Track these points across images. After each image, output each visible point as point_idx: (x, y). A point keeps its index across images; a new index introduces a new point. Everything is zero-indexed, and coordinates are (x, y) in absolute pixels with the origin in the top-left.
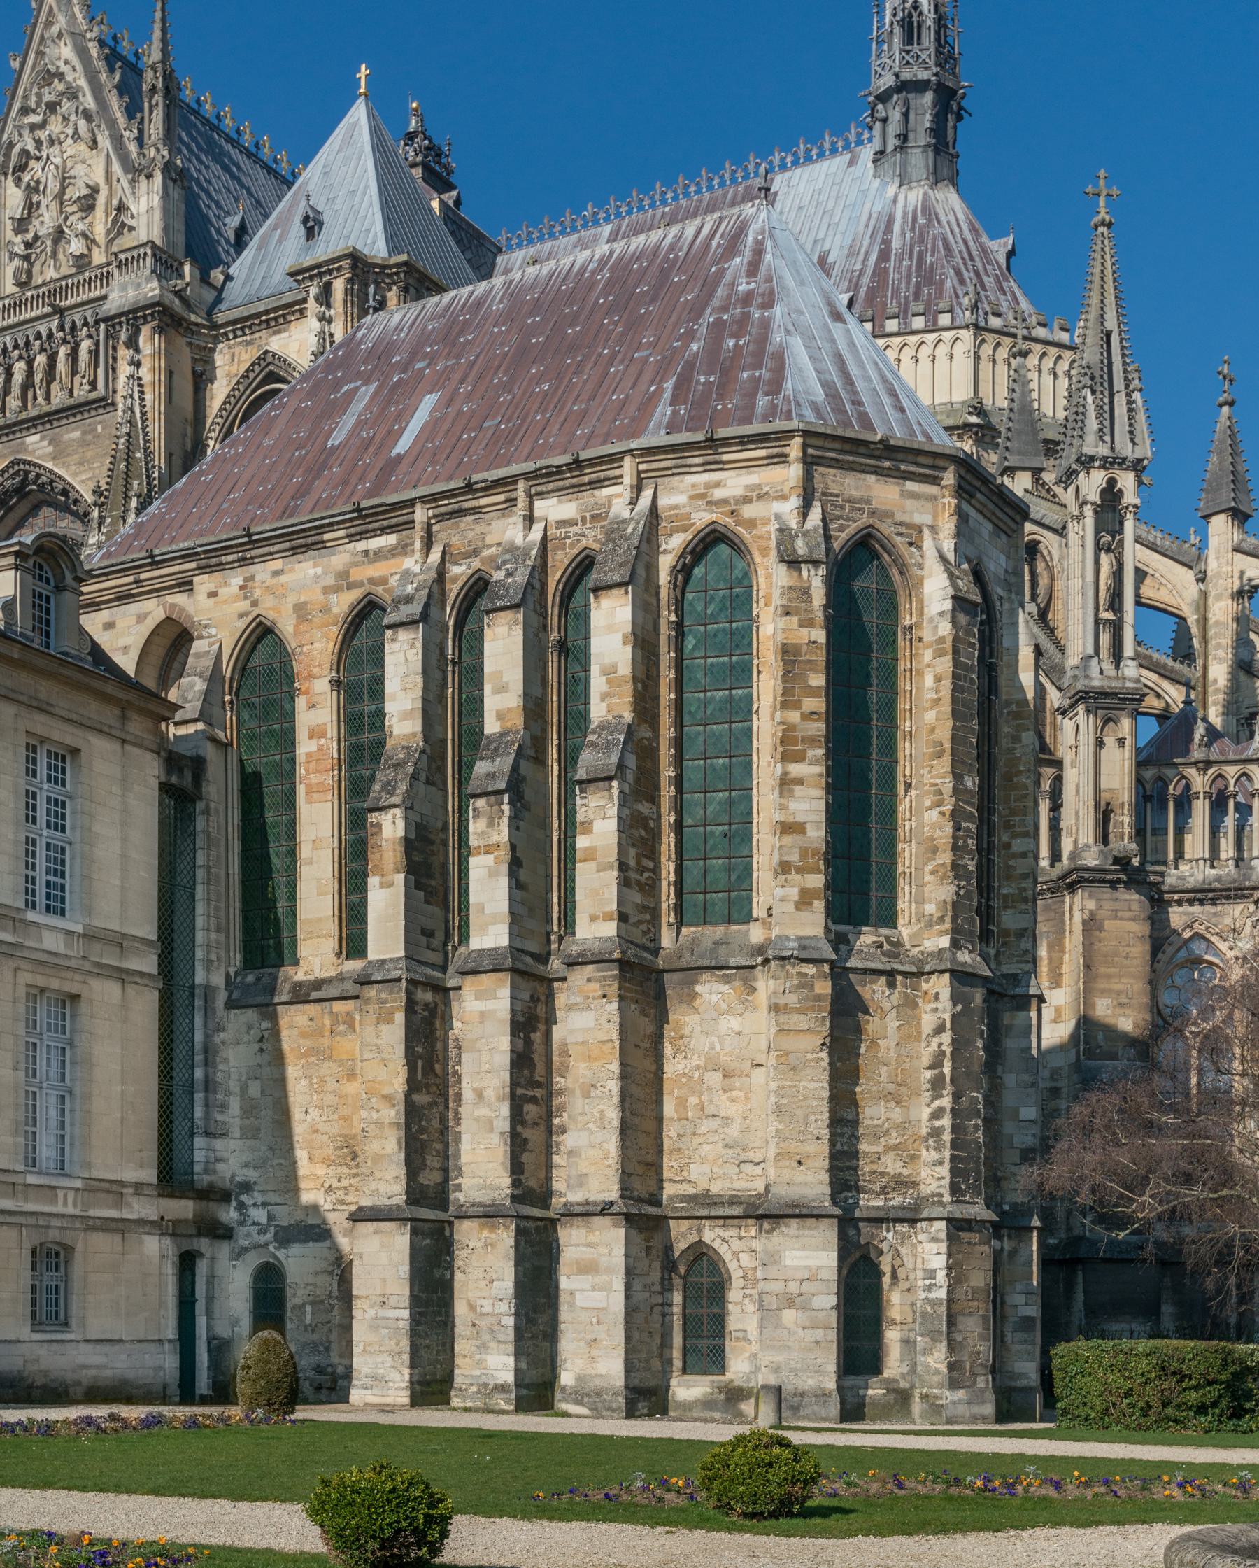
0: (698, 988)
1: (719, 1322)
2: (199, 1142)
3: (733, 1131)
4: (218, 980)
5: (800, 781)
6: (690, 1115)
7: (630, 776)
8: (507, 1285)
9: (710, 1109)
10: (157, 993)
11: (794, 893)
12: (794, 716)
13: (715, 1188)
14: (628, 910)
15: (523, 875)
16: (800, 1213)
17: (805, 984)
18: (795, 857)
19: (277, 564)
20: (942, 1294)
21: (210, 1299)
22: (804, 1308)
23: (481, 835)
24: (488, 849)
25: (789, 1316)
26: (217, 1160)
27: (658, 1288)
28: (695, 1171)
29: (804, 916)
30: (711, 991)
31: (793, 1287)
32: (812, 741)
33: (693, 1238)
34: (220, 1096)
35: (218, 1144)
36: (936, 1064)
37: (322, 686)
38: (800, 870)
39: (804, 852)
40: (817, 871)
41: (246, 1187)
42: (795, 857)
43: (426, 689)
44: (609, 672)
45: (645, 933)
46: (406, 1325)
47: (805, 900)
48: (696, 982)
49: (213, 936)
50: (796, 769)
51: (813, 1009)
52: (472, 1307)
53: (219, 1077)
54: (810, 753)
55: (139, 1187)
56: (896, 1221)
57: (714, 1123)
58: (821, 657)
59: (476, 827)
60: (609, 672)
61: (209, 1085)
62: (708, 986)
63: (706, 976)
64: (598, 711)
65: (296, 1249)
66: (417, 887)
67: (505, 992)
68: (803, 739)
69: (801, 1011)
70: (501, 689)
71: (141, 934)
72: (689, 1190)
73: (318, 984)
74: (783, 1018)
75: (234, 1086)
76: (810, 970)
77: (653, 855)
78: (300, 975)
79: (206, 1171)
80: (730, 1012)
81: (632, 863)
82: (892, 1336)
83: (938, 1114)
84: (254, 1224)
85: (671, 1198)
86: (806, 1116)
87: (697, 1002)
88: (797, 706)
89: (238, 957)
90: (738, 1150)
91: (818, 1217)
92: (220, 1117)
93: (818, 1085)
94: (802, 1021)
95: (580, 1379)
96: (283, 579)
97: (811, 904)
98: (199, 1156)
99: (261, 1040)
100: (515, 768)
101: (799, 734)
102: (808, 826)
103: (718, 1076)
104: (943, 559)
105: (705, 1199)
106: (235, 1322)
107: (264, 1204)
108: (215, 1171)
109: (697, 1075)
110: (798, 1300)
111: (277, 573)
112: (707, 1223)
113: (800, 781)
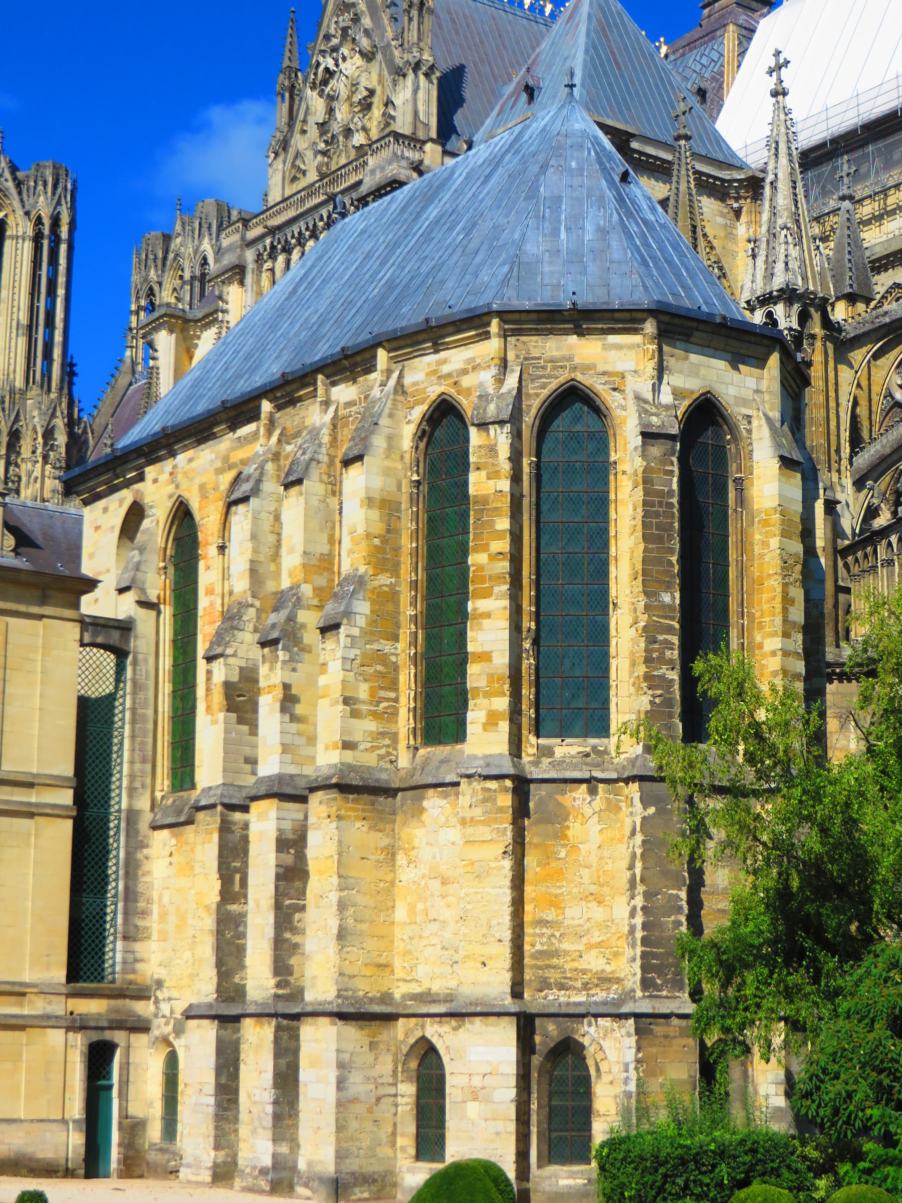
0: (425, 804)
2: (119, 945)
4: (143, 803)
5: (488, 615)
6: (418, 919)
7: (361, 621)
8: (269, 1076)
9: (433, 914)
10: (69, 824)
13: (437, 987)
14: (357, 737)
15: (299, 709)
17: (489, 798)
19: (190, 453)
20: (632, 1087)
21: (125, 1083)
22: (488, 1101)
23: (267, 677)
26: (136, 961)
27: (391, 1080)
28: (422, 972)
29: (491, 736)
31: (477, 1081)
32: (499, 578)
33: (419, 1034)
34: (141, 905)
35: (138, 946)
36: (631, 867)
38: (488, 695)
39: (491, 677)
40: (503, 694)
41: (159, 984)
43: (255, 551)
45: (381, 757)
46: (211, 1110)
48: (423, 798)
49: (138, 766)
51: (495, 820)
52: (249, 1096)
53: (141, 888)
54: (496, 589)
55: (44, 991)
56: (596, 1016)
57: (434, 927)
58: (505, 503)
59: (263, 670)
61: (131, 895)
62: (432, 801)
63: (431, 792)
66: (240, 721)
67: (273, 814)
68: (490, 577)
69: (483, 823)
70: (291, 551)
71: (56, 772)
72: (416, 989)
74: (470, 830)
75: (155, 897)
76: (493, 785)
77: (393, 685)
79: (124, 972)
83: (632, 914)
84: (163, 1016)
85: (403, 996)
86: (489, 920)
87: (424, 817)
88: (485, 548)
89: (167, 783)
90: (451, 952)
91: (499, 1015)
92: (140, 923)
93: (501, 891)
94: (484, 832)
95: (310, 1164)
96: (194, 464)
97: (497, 724)
98: (119, 957)
99: (171, 855)
101: (486, 573)
102: (494, 654)
103: (438, 882)
104: (638, 398)
105: (426, 997)
106: (150, 1105)
107: (170, 999)
108: (134, 971)
109: (423, 883)
110: (481, 1093)
111: (190, 460)
112: (428, 1020)
113: (488, 615)
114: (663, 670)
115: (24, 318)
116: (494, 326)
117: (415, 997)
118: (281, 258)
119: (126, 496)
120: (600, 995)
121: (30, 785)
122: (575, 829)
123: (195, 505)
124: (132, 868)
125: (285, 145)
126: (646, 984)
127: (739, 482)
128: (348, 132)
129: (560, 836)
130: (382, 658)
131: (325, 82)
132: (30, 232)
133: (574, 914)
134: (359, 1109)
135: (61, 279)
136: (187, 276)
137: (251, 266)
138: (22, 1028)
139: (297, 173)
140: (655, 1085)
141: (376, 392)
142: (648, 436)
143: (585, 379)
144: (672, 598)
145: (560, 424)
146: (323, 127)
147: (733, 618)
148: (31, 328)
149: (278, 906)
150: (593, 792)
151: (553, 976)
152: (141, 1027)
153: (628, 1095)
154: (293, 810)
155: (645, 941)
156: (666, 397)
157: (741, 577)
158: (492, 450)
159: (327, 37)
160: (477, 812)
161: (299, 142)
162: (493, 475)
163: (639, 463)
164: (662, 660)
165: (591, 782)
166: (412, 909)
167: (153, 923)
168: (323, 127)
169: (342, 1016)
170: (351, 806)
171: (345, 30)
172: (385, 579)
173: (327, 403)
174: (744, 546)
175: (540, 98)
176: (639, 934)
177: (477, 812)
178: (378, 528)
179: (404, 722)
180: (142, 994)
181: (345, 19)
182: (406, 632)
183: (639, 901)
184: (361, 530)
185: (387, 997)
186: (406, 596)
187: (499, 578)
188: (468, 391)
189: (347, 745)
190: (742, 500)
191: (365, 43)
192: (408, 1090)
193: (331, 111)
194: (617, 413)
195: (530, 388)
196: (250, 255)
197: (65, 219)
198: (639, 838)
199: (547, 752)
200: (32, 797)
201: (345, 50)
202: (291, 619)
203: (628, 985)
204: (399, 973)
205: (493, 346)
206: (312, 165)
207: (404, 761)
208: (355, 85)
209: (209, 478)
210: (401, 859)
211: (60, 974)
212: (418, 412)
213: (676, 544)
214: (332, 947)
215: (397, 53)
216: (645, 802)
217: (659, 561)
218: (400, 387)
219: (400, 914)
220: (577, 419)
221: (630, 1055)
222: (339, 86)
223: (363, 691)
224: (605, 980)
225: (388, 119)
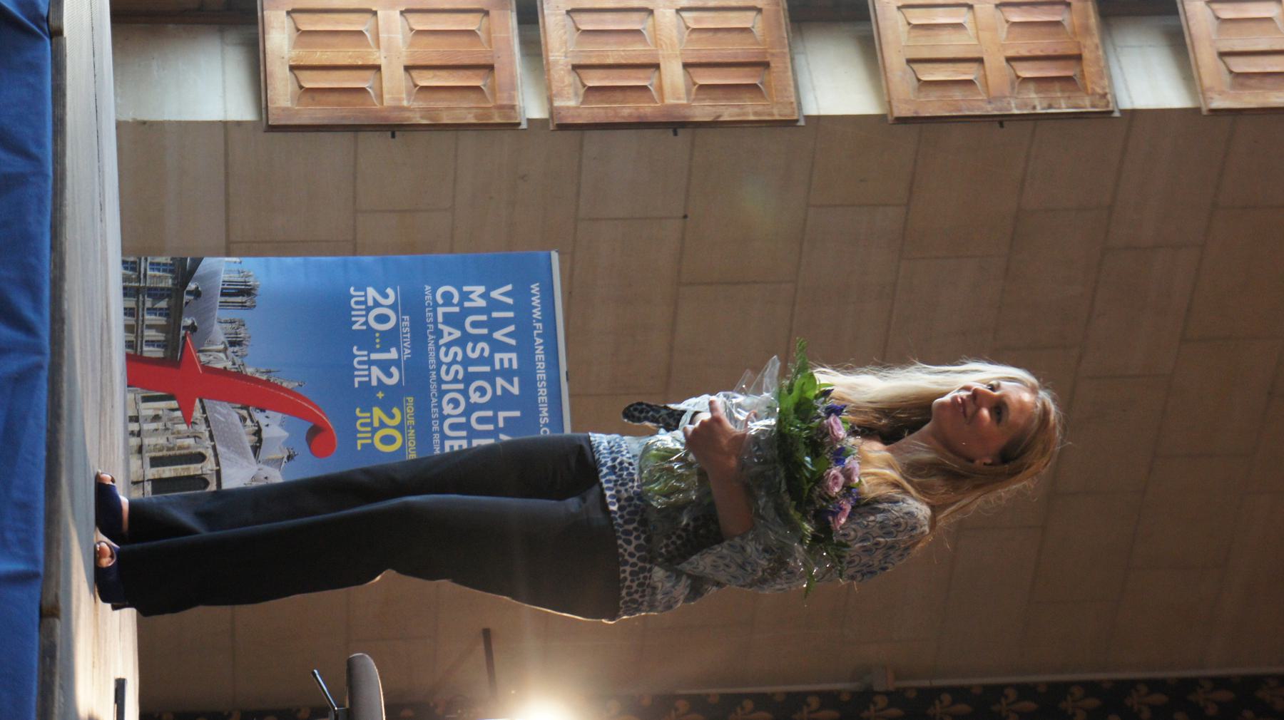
47: (153, 475)
50: (172, 471)
179: (153, 454)
218: (207, 448)
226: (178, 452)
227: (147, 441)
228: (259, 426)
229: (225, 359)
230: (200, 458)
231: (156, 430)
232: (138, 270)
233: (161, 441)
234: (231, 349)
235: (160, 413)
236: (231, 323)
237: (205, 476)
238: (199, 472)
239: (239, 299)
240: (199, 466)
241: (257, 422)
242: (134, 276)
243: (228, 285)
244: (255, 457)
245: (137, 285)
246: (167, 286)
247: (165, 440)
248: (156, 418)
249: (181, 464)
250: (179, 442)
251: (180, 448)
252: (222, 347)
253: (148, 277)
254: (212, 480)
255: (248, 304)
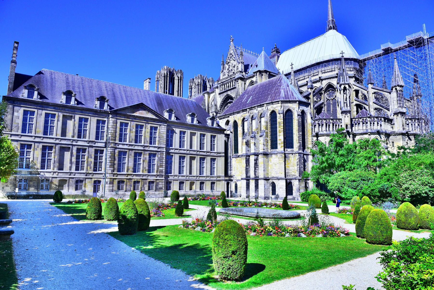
1: (275, 190)
3: (276, 170)
4: (231, 155)
7: (265, 135)
11: (280, 146)
12: (280, 129)
13: (274, 176)
15: (256, 145)
16: (282, 179)
17: (282, 155)
18: (280, 143)
21: (230, 187)
22: (282, 188)
24: (252, 143)
25: (281, 189)
28: (272, 174)
30: (273, 156)
31: (281, 186)
32: (282, 131)
35: (231, 171)
37: (240, 126)
39: (281, 142)
41: (234, 176)
42: (280, 143)
44: (263, 125)
47: (281, 147)
50: (280, 134)
58: (282, 123)
59: (251, 141)
60: (263, 125)
61: (230, 166)
64: (262, 129)
65: (238, 182)
73: (240, 156)
77: (268, 143)
78: (239, 154)
80: (275, 158)
81: (265, 144)
82: (294, 191)
83: (297, 168)
94: (281, 159)
98: (229, 173)
100: (255, 135)
114: (300, 141)
115: (177, 90)
116: (280, 102)
117: (272, 177)
118: (223, 86)
119: (226, 119)
120: (294, 177)
121: (220, 153)
122: (290, 159)
123: (237, 121)
124: (230, 162)
125: (223, 71)
126: (299, 176)
127: (306, 120)
128: (232, 70)
129: (289, 159)
130: (267, 140)
131: (228, 64)
132: (178, 79)
133: (291, 168)
134: (266, 189)
135: (182, 85)
136: (197, 84)
137: (219, 87)
138: (220, 181)
139: (224, 75)
140: (300, 187)
141: (264, 109)
142: (298, 115)
143: (291, 108)
144: (301, 133)
145: (287, 114)
146: (228, 69)
147: (306, 135)
148: (178, 91)
149: (255, 167)
150: (292, 155)
151: (288, 175)
152: (232, 180)
153: (298, 188)
154: (256, 157)
155: (299, 171)
156: (300, 111)
157: (306, 130)
158: (281, 116)
159: (228, 58)
160: (280, 157)
161: (224, 71)
162: (281, 119)
163: (297, 118)
164: (300, 140)
165: (292, 154)
166: (271, 167)
167: (233, 169)
168: (228, 69)
169: (265, 180)
170: (265, 156)
171: (231, 57)
172: (267, 131)
173: (257, 110)
174: (307, 127)
175: (258, 67)
176: (298, 170)
177: (280, 157)
178: (266, 125)
179: (269, 147)
180: (232, 177)
181: (231, 56)
182: (269, 136)
183: (298, 167)
184: (264, 125)
185: (268, 177)
186: (269, 132)
187: (282, 131)
188: (276, 110)
189: (264, 149)
190: (306, 122)
191: (234, 59)
192: (271, 187)
193: (229, 67)
194: (294, 112)
195: (284, 110)
196: (219, 85)
197: (182, 77)
198: (298, 160)
199: (287, 150)
200: (220, 154)
201: (231, 59)
202: (255, 135)
203: (297, 176)
204: (269, 174)
205: (280, 105)
206: (227, 74)
207: (269, 151)
208: (232, 64)
209: (239, 118)
210: (269, 162)
211: (224, 175)
212: (270, 112)
213: (301, 127)
214: (263, 172)
215: (239, 60)
216: (299, 156)
217: (300, 129)
218: (267, 109)
219: (269, 168)
220: (289, 113)
221: (298, 184)
222: (230, 64)
223: (265, 144)
224: (294, 175)
225: (237, 69)
226: (269, 130)
227: (261, 151)
228: (256, 72)
229: (214, 94)
230: (273, 114)
231: (255, 144)
232: (155, 153)
233: (261, 140)
234: (208, 90)
235: (245, 141)
236: (191, 88)
237: (285, 111)
238: (282, 115)
239: (176, 82)
240: (278, 115)
241: (254, 73)
242: (159, 156)
243: (167, 90)
244: (275, 76)
245: (164, 153)
246: (165, 133)
247: (261, 138)
248: (248, 144)
249: (276, 128)
250: (263, 128)
251: (267, 128)
252: (206, 95)
253: (159, 146)
254: (287, 107)
255: (179, 76)
